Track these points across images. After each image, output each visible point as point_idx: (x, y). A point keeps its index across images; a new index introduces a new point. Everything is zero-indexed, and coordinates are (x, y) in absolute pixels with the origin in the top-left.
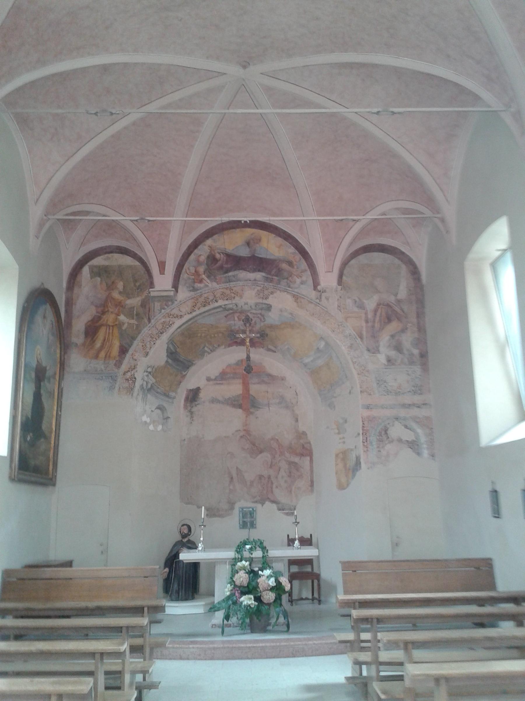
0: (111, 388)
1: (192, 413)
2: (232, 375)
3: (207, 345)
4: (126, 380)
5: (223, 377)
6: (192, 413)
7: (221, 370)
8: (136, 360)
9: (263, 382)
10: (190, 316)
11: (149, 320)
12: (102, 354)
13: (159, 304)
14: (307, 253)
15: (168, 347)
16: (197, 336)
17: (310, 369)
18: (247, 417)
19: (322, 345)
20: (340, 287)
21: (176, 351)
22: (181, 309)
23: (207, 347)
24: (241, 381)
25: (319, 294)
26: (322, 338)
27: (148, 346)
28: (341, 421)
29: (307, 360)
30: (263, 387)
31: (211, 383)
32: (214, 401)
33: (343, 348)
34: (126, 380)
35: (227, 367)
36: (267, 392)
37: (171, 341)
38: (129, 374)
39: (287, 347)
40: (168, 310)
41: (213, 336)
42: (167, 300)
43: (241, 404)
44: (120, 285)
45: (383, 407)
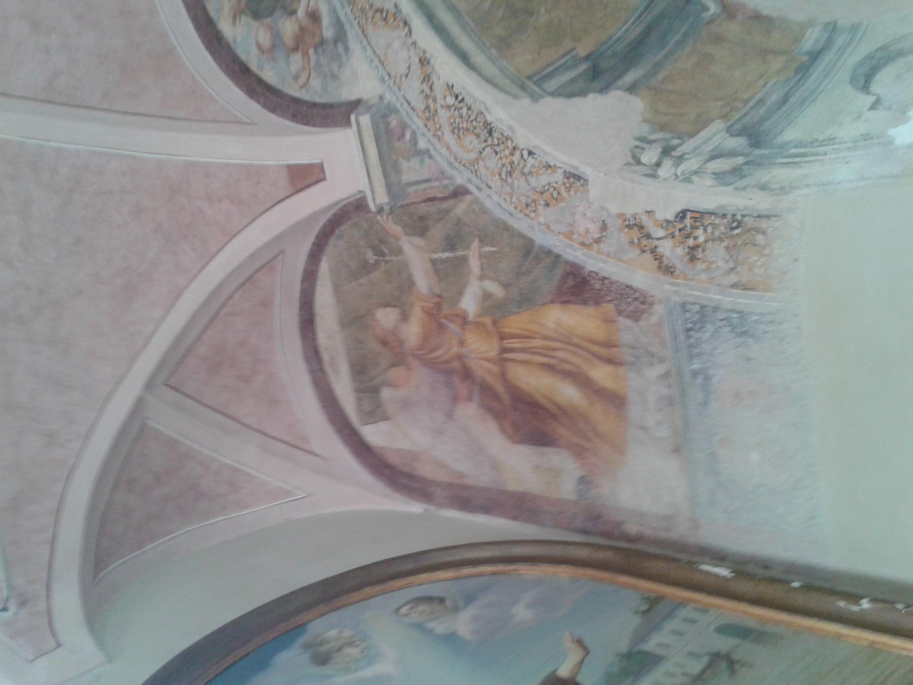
0: (741, 326)
4: (693, 259)
8: (604, 227)
10: (418, 23)
11: (459, 193)
12: (601, 374)
13: (405, 165)
21: (587, 58)
22: (403, 70)
27: (544, 179)
34: (693, 259)
37: (533, 84)
38: (666, 248)
40: (417, 123)
42: (390, 139)
44: (386, 317)
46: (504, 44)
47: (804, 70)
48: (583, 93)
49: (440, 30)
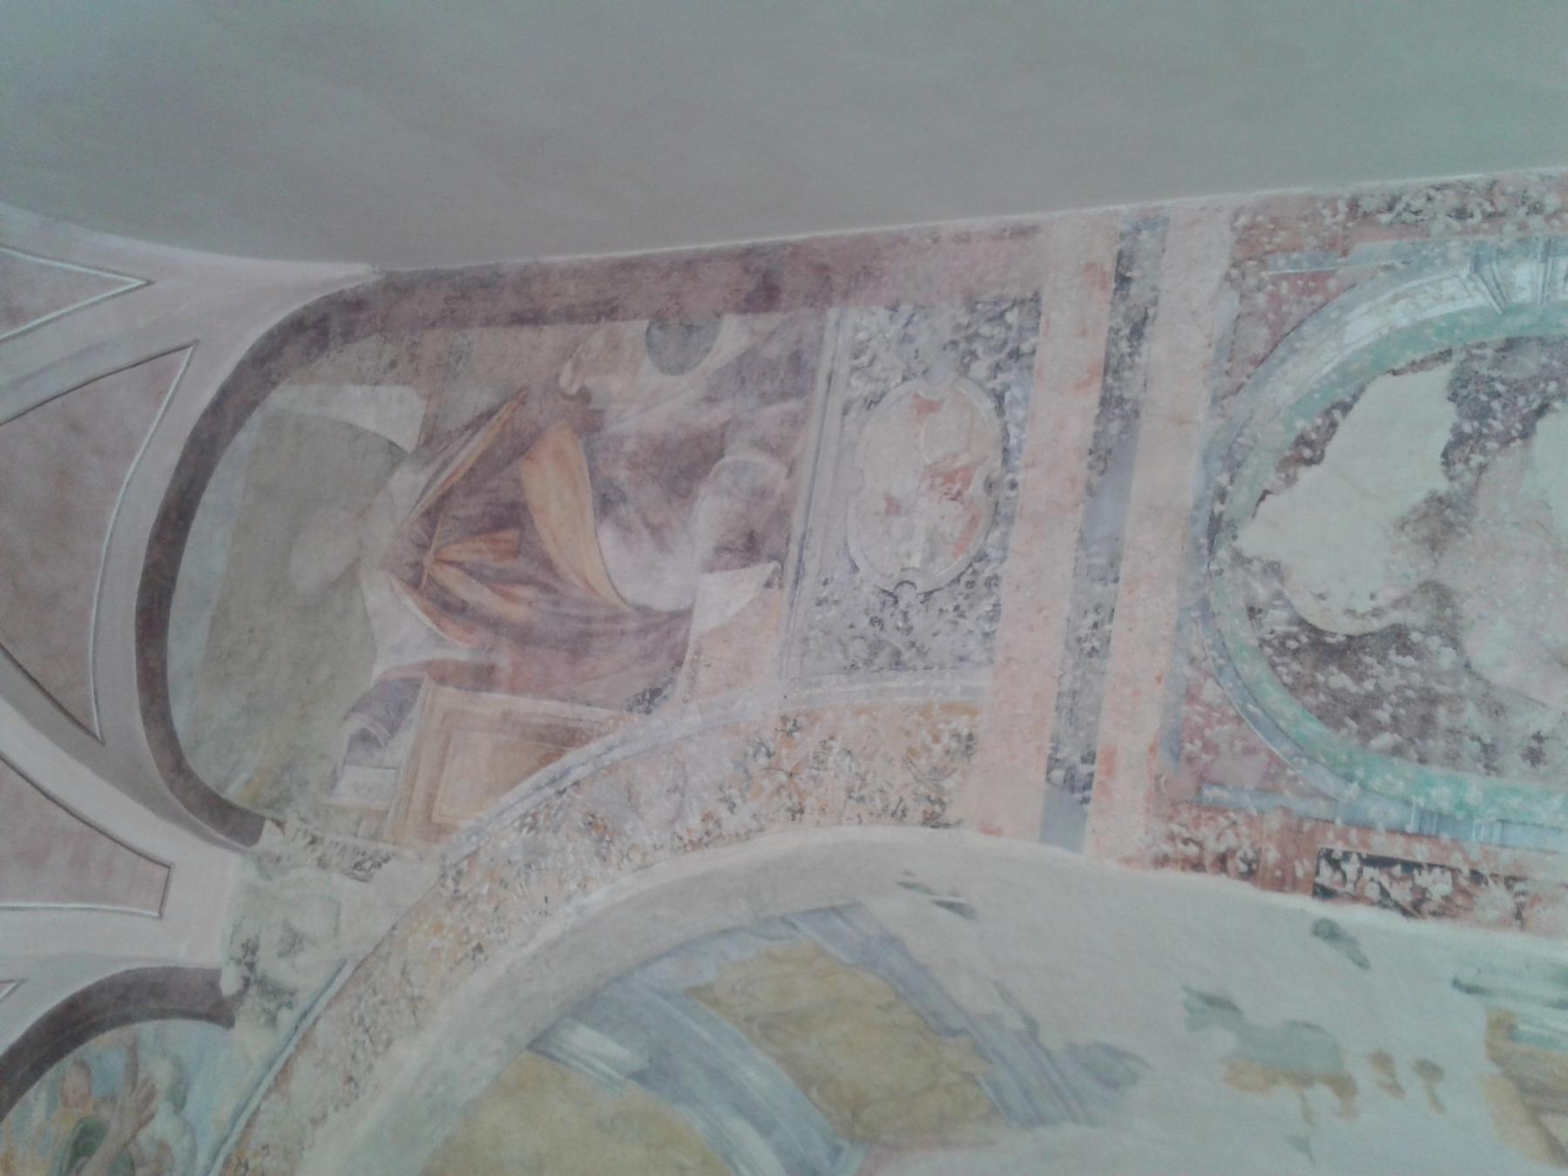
14: (72, 1005)
17: (838, 1150)
20: (270, 837)
25: (253, 999)
26: (540, 1044)
28: (1223, 1040)
33: (597, 897)
45: (1090, 649)
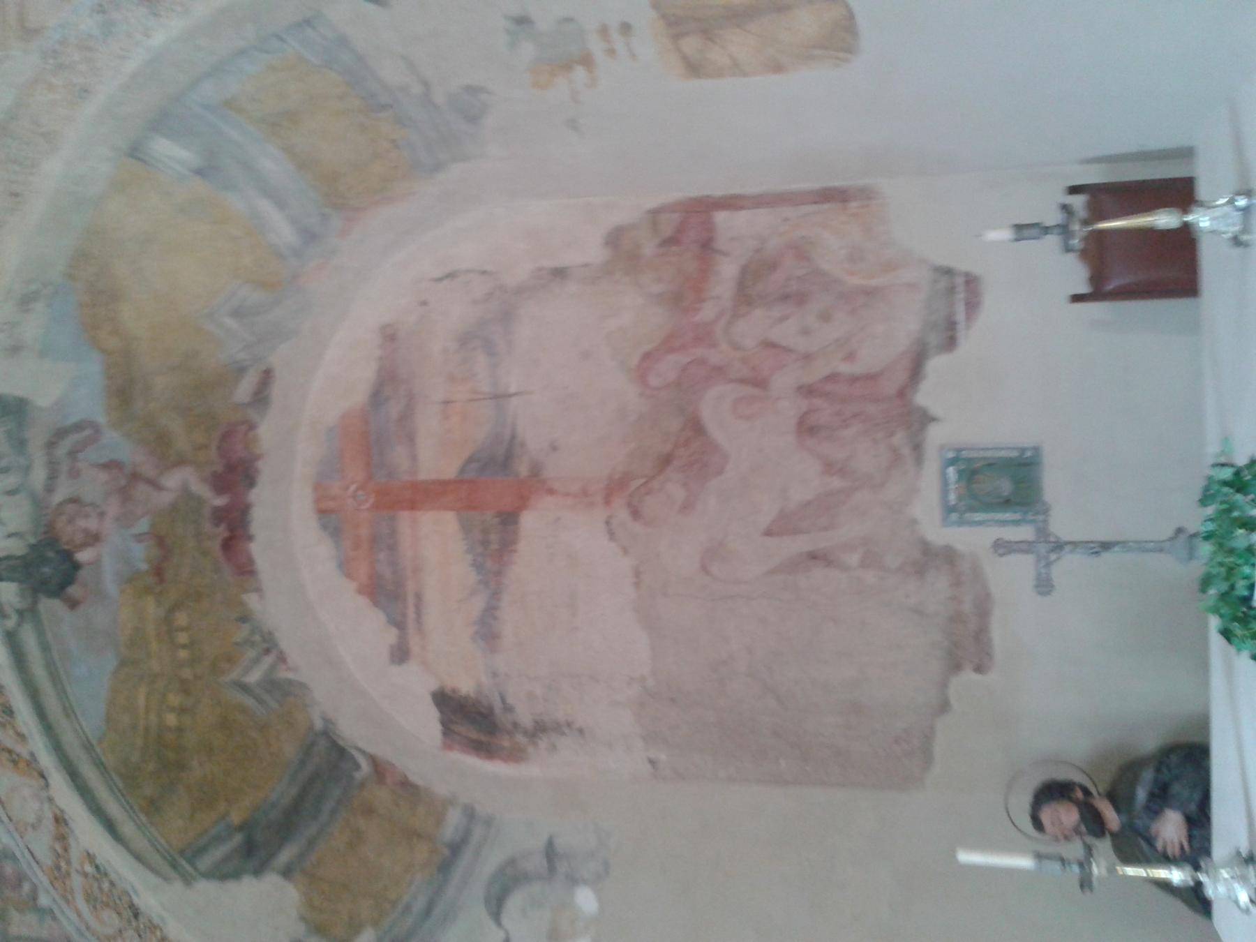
1: (540, 729)
2: (382, 556)
3: (234, 675)
5: (388, 591)
6: (540, 729)
7: (363, 602)
9: (406, 416)
10: (59, 782)
13: (14, 915)
15: (208, 875)
16: (180, 730)
18: (551, 492)
19: (170, 151)
21: (240, 828)
22: (31, 818)
23: (247, 670)
24: (404, 517)
28: (528, 50)
29: (283, 232)
30: (428, 423)
31: (414, 642)
32: (487, 632)
33: (158, 39)
35: (349, 576)
36: (447, 402)
37: (183, 862)
39: (230, 322)
41: (183, 654)
43: (499, 514)
46: (153, 807)
47: (445, 868)
48: (236, 875)
49: (83, 790)
